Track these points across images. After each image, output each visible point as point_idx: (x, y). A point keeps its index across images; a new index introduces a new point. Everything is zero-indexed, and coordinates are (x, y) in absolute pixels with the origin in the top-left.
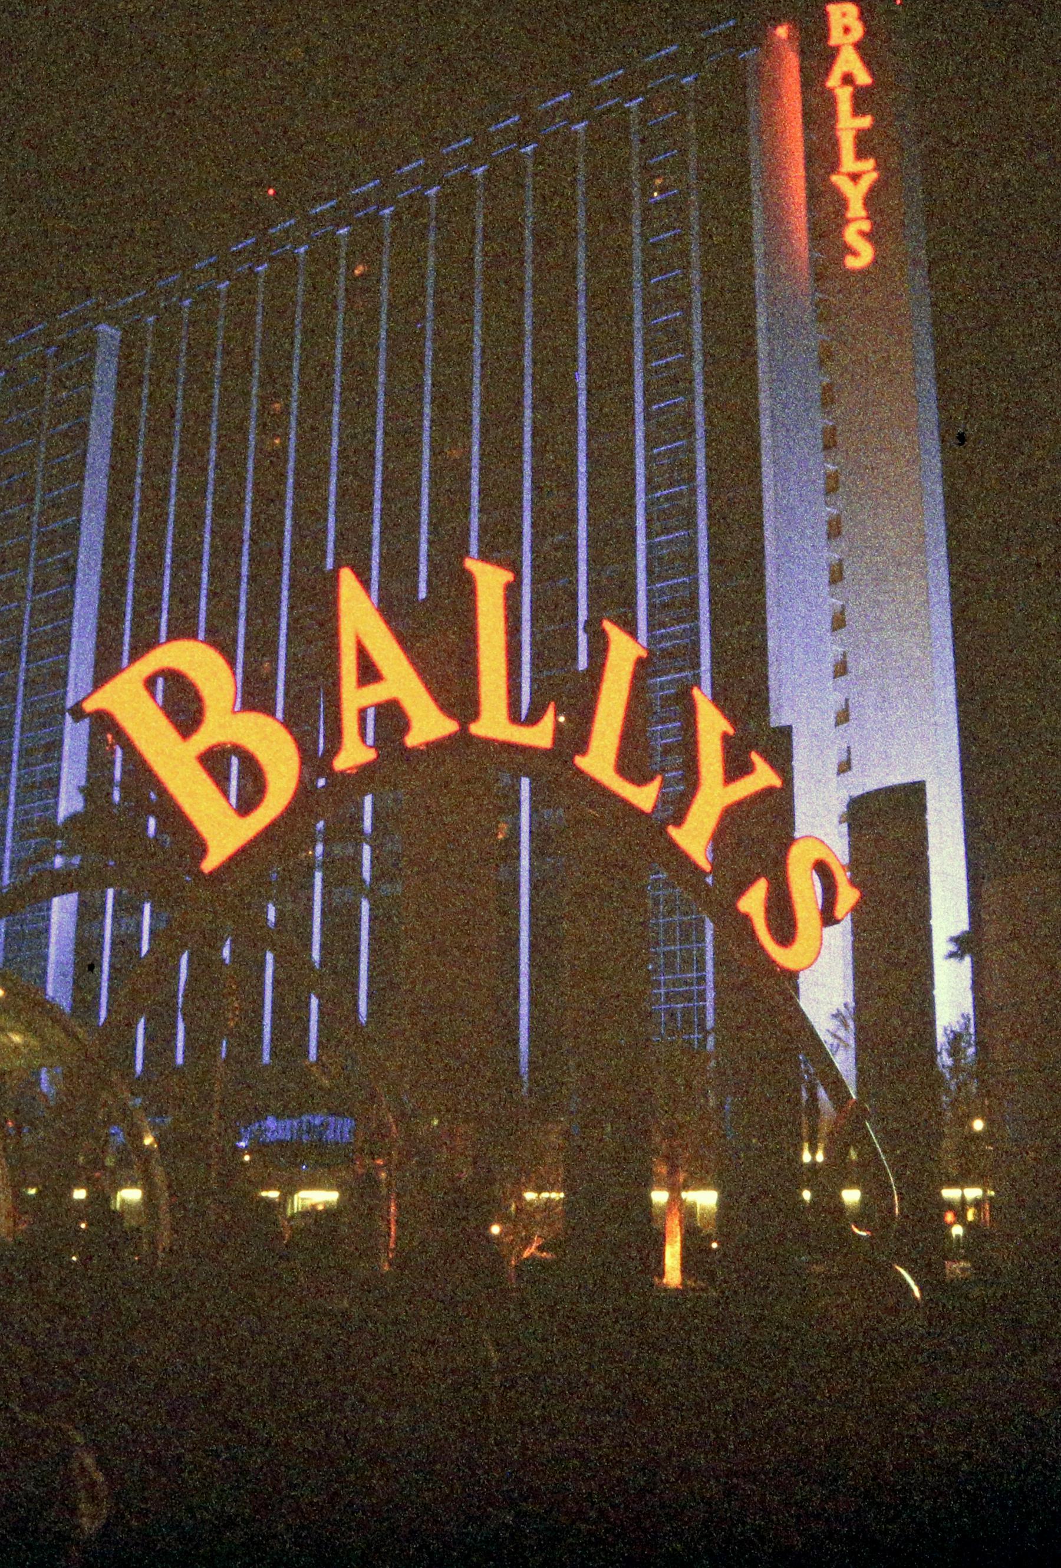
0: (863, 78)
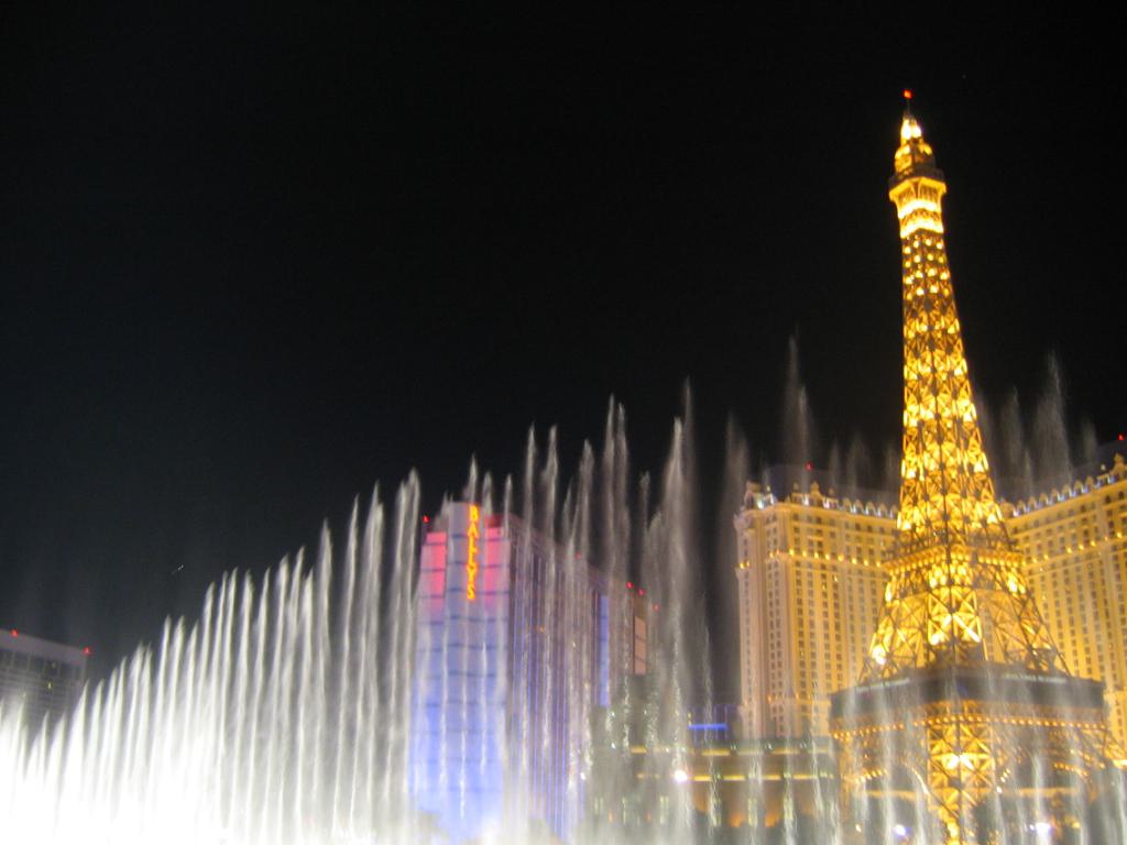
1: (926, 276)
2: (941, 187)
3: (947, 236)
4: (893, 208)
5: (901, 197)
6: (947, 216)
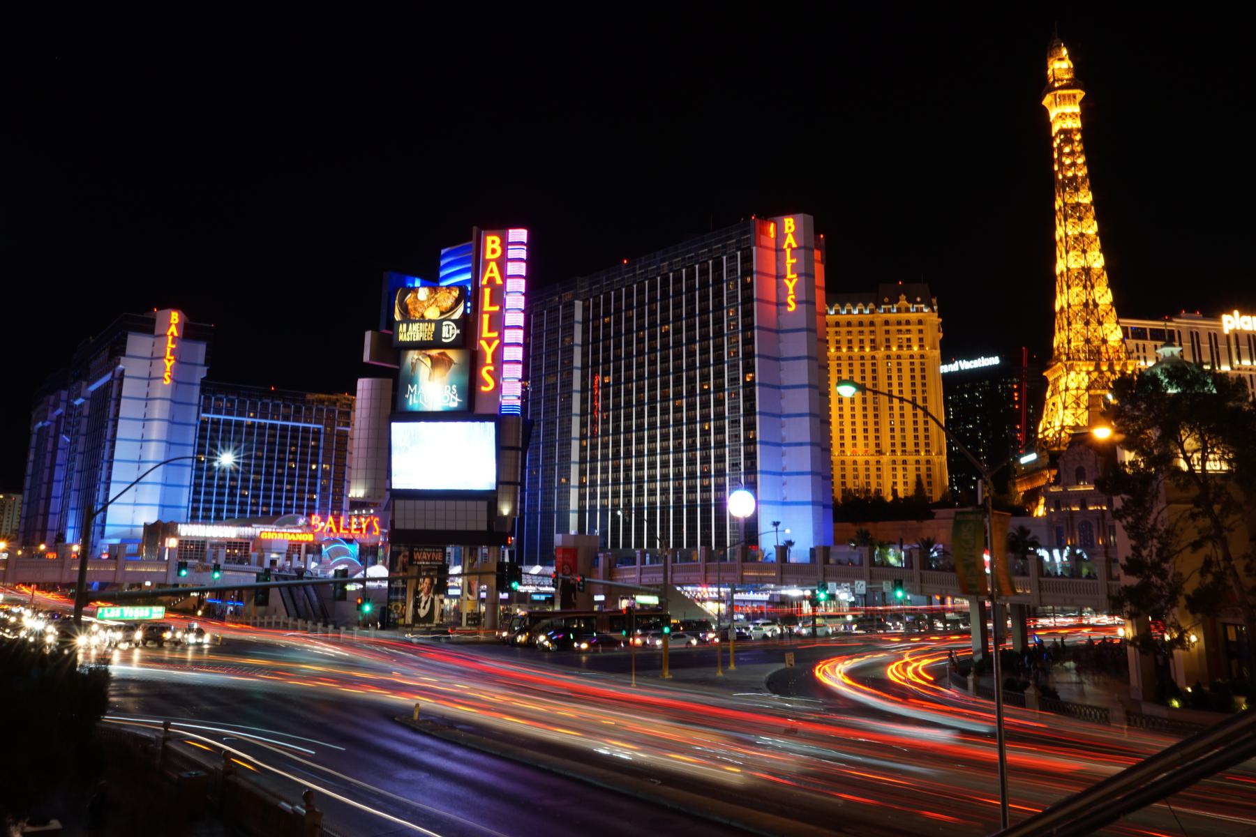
0: (794, 245)
1: (1072, 163)
2: (1080, 94)
3: (1082, 131)
4: (1045, 112)
5: (1051, 104)
6: (1083, 117)
